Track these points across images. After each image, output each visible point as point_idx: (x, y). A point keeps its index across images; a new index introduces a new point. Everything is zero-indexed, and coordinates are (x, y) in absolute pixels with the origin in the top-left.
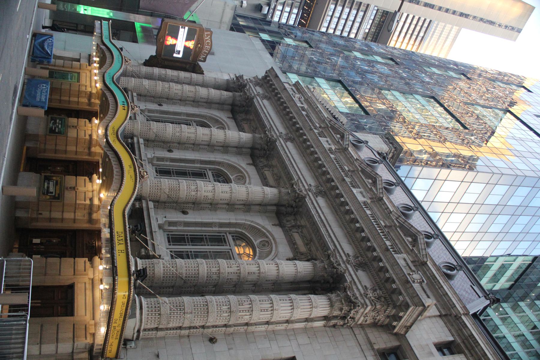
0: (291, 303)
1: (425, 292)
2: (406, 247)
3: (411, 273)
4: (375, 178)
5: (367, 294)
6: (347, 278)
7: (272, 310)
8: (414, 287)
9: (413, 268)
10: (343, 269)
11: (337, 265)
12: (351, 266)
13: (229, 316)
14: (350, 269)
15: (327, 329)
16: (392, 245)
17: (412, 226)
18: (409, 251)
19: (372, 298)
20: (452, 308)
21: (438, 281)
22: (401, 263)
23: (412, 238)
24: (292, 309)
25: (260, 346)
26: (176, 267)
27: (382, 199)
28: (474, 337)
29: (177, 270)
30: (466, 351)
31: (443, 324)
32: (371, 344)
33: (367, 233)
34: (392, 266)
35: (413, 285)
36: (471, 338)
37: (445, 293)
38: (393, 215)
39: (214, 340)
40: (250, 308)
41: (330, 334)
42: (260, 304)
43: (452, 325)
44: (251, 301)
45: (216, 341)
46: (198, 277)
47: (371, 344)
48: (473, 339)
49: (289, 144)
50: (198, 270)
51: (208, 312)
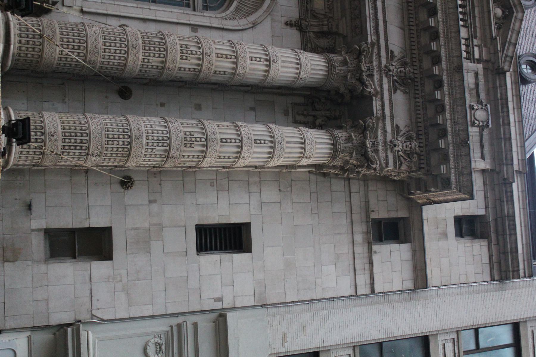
0: (271, 147)
1: (482, 146)
2: (487, 27)
3: (475, 108)
5: (395, 145)
6: (374, 103)
7: (236, 157)
8: (470, 134)
9: (482, 96)
10: (375, 89)
11: (367, 76)
12: (389, 82)
13: (163, 161)
14: (386, 87)
15: (313, 177)
16: (466, 39)
18: (488, 36)
19: (401, 153)
20: (507, 165)
21: (508, 112)
22: (469, 80)
23: (503, 12)
24: (269, 158)
25: (201, 200)
26: (86, 48)
28: (514, 220)
29: (86, 55)
30: (493, 236)
31: (483, 185)
32: (368, 211)
33: (438, 22)
34: (453, 103)
35: (470, 129)
36: (509, 220)
37: (507, 136)
39: (130, 184)
40: (202, 151)
41: (313, 186)
42: (221, 146)
43: (493, 189)
44: (206, 140)
45: (131, 187)
46: (123, 70)
47: (368, 211)
48: (511, 223)
50: (126, 59)
51: (129, 155)
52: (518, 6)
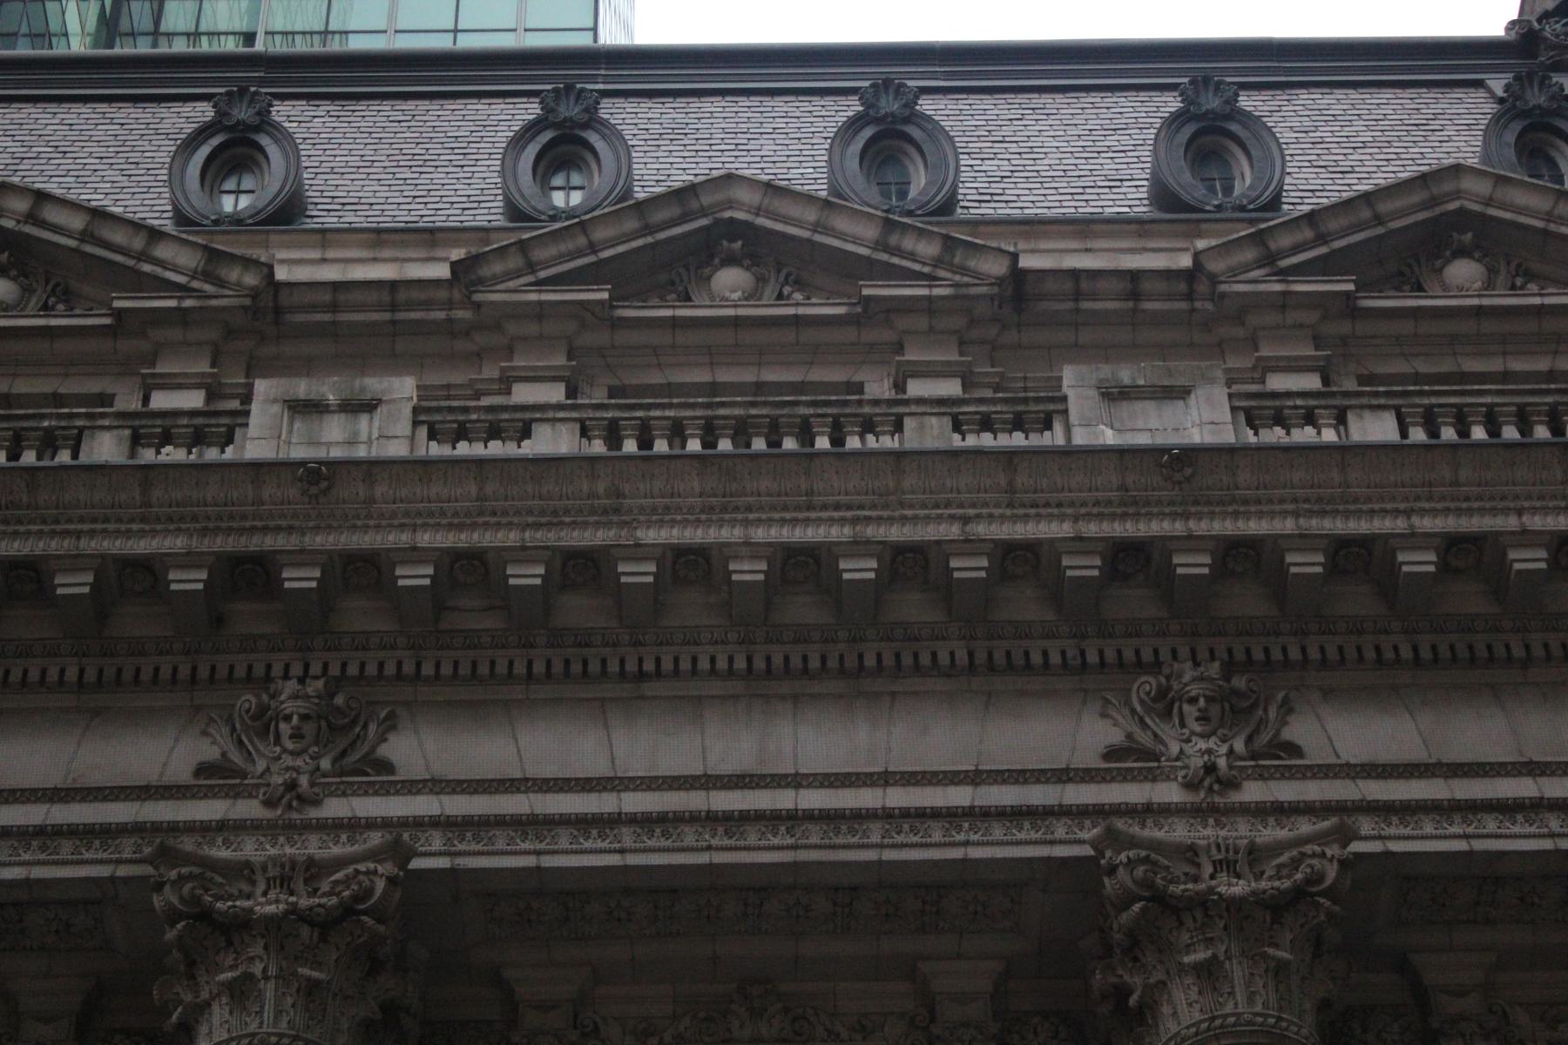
4: (735, 229)
17: (1366, 197)
23: (1462, 252)
27: (1018, 276)
38: (1235, 272)
49: (407, 750)
52: (1435, 191)
